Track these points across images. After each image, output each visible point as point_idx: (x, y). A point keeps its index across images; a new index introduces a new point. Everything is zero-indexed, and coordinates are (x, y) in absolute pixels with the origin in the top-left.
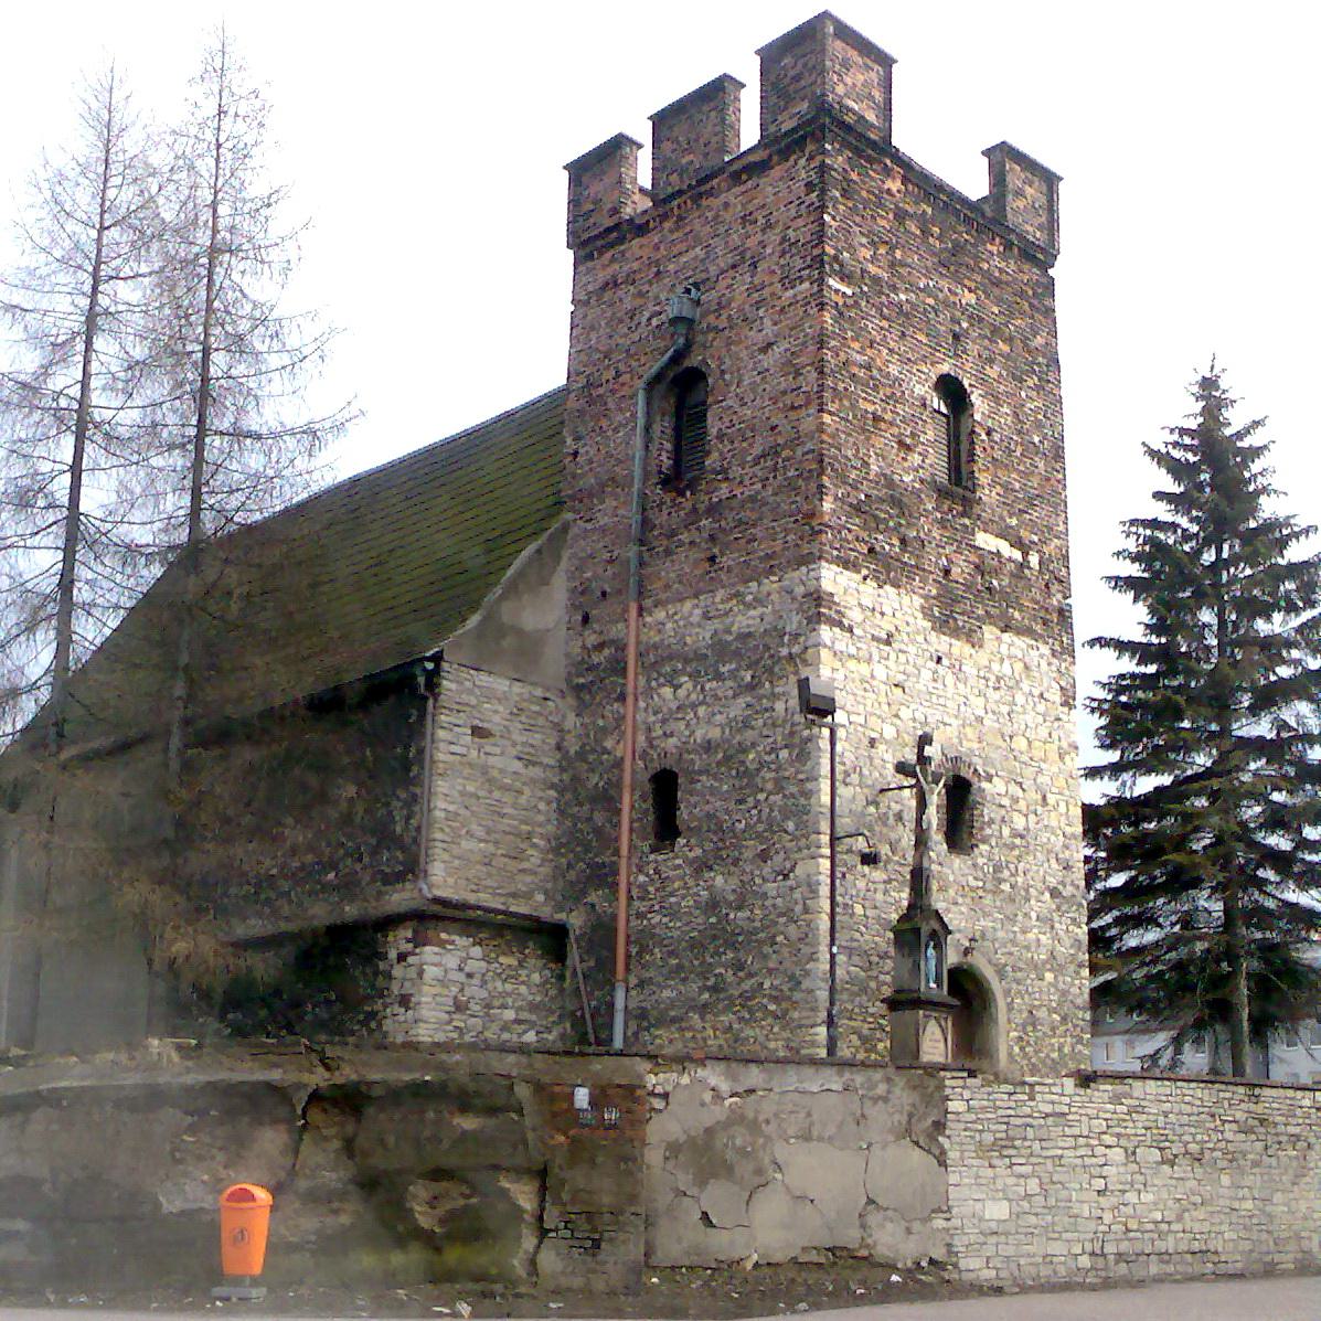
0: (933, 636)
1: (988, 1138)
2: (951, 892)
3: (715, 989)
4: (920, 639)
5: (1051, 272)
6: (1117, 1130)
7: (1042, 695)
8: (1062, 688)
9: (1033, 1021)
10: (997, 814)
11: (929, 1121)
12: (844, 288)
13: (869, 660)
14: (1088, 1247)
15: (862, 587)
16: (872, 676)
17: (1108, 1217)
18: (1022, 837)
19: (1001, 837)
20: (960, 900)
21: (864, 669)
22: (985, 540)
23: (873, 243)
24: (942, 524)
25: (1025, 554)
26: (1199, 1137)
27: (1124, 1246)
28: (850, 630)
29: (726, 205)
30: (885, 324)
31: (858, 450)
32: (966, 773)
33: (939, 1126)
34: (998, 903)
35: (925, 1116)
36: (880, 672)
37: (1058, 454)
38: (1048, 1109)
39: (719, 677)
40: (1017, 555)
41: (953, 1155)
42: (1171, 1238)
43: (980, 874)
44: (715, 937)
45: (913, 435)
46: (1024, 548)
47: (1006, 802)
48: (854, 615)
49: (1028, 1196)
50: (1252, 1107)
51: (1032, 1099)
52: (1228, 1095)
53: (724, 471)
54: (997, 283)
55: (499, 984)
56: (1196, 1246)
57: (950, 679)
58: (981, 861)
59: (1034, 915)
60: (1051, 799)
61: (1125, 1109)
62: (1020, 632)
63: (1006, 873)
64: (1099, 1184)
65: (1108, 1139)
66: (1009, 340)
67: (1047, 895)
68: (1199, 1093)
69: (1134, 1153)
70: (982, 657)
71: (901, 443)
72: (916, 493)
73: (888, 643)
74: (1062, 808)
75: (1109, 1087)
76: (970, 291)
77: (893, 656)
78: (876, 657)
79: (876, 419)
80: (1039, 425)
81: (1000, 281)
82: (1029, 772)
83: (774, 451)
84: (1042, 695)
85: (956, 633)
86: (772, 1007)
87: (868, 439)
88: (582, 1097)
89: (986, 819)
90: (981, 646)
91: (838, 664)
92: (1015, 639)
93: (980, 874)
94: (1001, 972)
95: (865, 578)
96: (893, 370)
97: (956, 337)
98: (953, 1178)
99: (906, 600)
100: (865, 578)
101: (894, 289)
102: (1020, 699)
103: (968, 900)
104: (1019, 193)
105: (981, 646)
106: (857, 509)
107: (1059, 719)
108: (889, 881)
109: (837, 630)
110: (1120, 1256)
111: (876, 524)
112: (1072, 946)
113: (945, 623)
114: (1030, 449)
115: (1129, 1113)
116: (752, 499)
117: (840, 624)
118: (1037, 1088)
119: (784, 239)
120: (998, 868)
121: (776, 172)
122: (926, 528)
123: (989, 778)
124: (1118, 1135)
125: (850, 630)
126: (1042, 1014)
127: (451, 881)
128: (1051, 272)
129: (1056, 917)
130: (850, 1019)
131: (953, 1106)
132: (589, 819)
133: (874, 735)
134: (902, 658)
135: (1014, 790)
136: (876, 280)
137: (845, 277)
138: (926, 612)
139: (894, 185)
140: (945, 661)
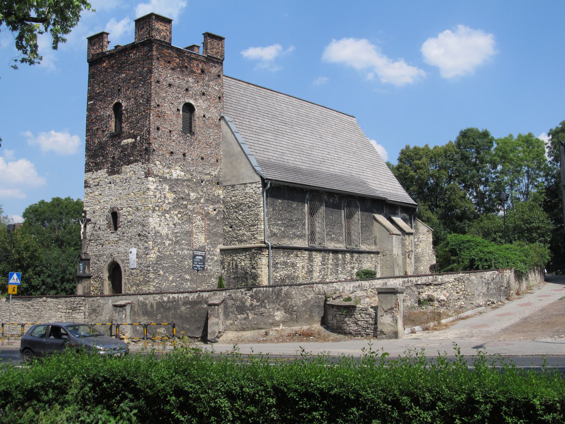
0: (109, 178)
21: (93, 195)
40: (134, 140)
72: (107, 142)
73: (98, 185)
79: (97, 129)
92: (132, 166)
120: (123, 233)
123: (122, 209)
136: (99, 93)
140: (112, 182)
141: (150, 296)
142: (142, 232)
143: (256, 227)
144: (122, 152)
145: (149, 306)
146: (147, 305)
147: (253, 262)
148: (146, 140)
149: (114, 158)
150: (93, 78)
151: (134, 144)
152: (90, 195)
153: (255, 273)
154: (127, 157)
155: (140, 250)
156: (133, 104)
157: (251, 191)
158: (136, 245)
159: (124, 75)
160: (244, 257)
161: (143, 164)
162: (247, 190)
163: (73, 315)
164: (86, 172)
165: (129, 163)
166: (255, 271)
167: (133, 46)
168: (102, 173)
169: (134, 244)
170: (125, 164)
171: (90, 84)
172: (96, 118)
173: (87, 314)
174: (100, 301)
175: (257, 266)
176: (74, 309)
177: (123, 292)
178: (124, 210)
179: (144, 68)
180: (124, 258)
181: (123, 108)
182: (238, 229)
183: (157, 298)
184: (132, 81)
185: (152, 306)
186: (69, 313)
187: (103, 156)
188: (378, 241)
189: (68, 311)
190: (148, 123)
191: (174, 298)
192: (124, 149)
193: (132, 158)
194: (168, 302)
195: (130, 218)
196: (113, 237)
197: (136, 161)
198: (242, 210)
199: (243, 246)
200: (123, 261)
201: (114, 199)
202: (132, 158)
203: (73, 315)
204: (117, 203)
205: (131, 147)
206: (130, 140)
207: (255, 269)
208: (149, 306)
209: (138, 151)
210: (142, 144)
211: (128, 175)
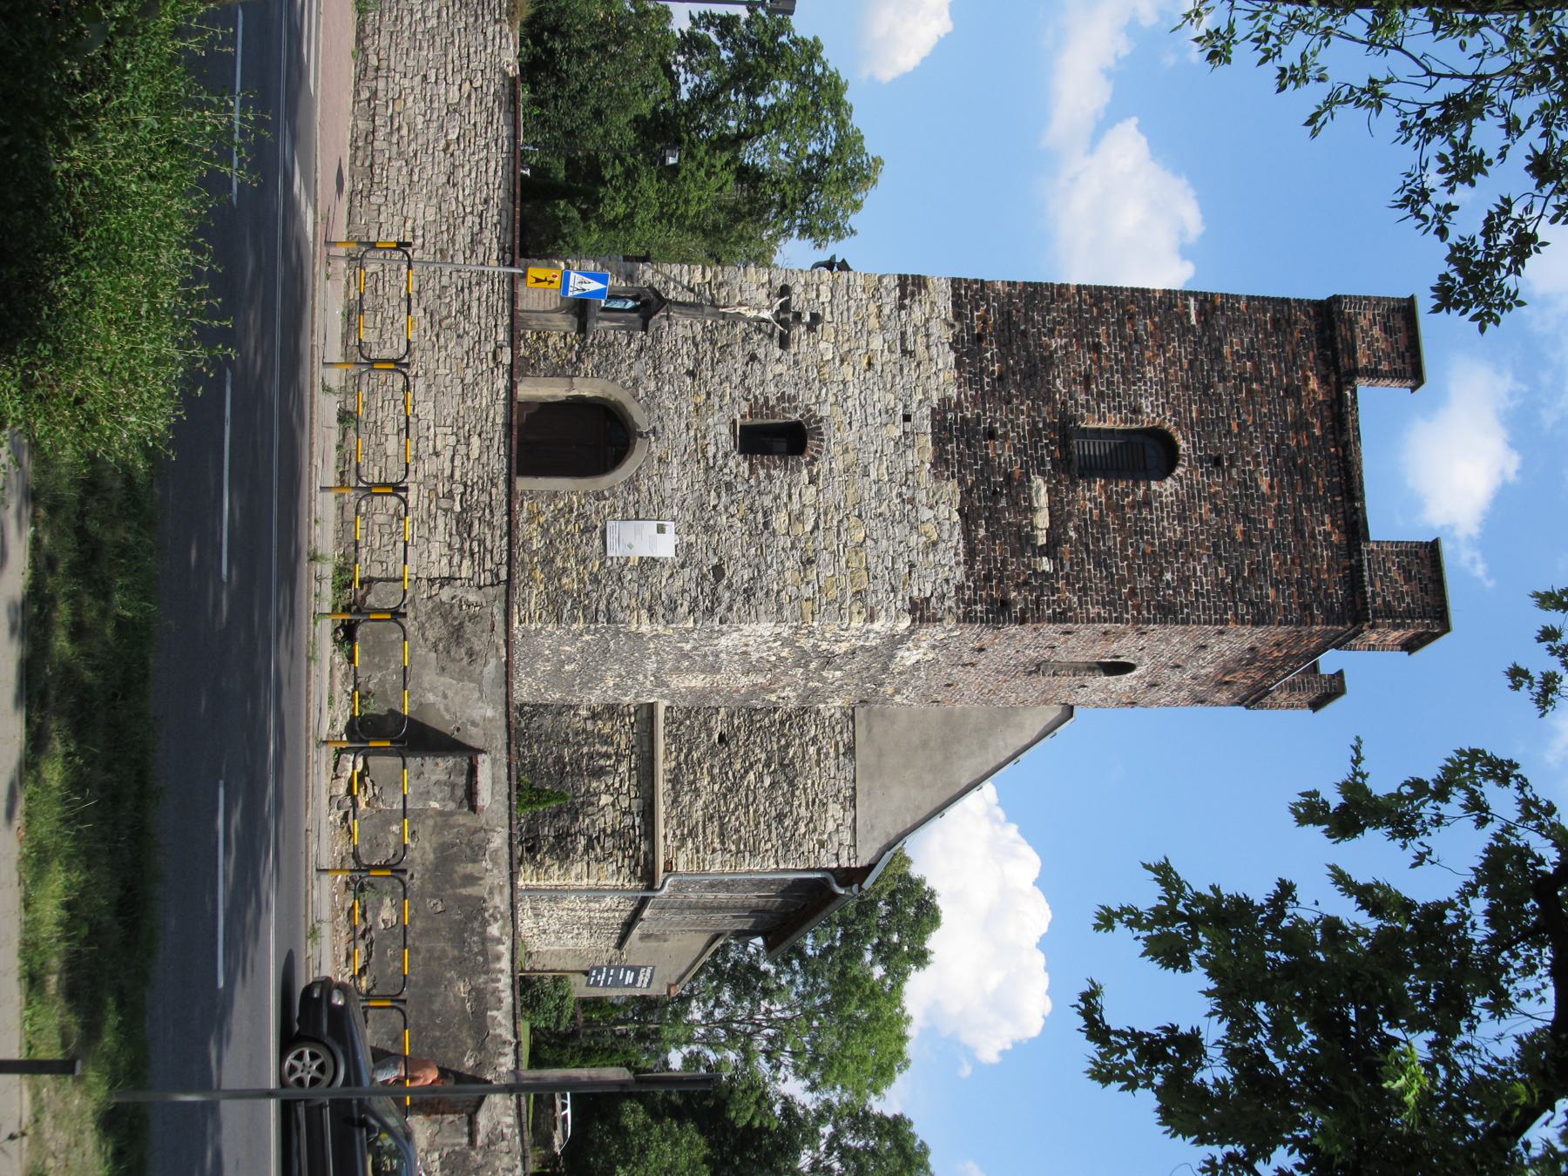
0: (926, 411)
13: (882, 328)
17: (406, 83)
18: (766, 525)
20: (692, 433)
21: (873, 322)
22: (1039, 484)
24: (1035, 431)
25: (1050, 550)
28: (902, 307)
31: (1059, 323)
40: (1042, 541)
42: (385, 145)
45: (1101, 394)
46: (1050, 550)
47: (795, 506)
54: (1299, 532)
59: (693, 538)
62: (967, 534)
65: (467, 86)
67: (715, 561)
70: (925, 476)
72: (1048, 398)
73: (905, 352)
78: (888, 336)
79: (1096, 348)
80: (1184, 581)
81: (1303, 536)
85: (937, 441)
89: (775, 473)
92: (958, 529)
100: (952, 326)
101: (1223, 379)
108: (696, 345)
110: (374, 94)
111: (1005, 345)
113: (938, 416)
117: (903, 296)
120: (729, 486)
125: (902, 307)
136: (1219, 354)
138: (944, 401)
140: (908, 426)
141: (506, 873)
142: (729, 587)
143: (717, 846)
144: (1009, 477)
145: (470, 868)
146: (475, 861)
147: (609, 843)
148: (1037, 602)
149: (991, 434)
150: (1275, 321)
151: (1023, 541)
152: (873, 308)
153: (574, 850)
154: (988, 505)
155: (666, 574)
156: (1162, 535)
157: (831, 826)
158: (686, 551)
159: (1264, 488)
160: (625, 804)
162: (835, 810)
163: (441, 521)
164: (956, 283)
165: (968, 517)
166: (581, 848)
167: (1355, 527)
168: (940, 375)
169: (690, 545)
170: (967, 493)
171: (1260, 303)
172: (1138, 339)
173: (445, 594)
174: (493, 662)
175: (597, 860)
176: (463, 525)
177: (522, 484)
179: (1275, 584)
180: (644, 489)
181: (1154, 485)
182: (716, 771)
183: (497, 900)
184: (1239, 527)
185: (471, 880)
186: (450, 495)
187: (1000, 378)
188: (653, 944)
190: (1093, 611)
191: (498, 958)
192: (1016, 487)
193: (982, 532)
194: (485, 939)
195: (780, 521)
196: (721, 435)
197: (971, 553)
198: (773, 785)
199: (662, 786)
200: (632, 484)
201: (850, 437)
205: (1020, 527)
206: (1042, 520)
207: (586, 851)
208: (470, 868)
209: (1004, 562)
210: (1026, 583)
211: (926, 514)
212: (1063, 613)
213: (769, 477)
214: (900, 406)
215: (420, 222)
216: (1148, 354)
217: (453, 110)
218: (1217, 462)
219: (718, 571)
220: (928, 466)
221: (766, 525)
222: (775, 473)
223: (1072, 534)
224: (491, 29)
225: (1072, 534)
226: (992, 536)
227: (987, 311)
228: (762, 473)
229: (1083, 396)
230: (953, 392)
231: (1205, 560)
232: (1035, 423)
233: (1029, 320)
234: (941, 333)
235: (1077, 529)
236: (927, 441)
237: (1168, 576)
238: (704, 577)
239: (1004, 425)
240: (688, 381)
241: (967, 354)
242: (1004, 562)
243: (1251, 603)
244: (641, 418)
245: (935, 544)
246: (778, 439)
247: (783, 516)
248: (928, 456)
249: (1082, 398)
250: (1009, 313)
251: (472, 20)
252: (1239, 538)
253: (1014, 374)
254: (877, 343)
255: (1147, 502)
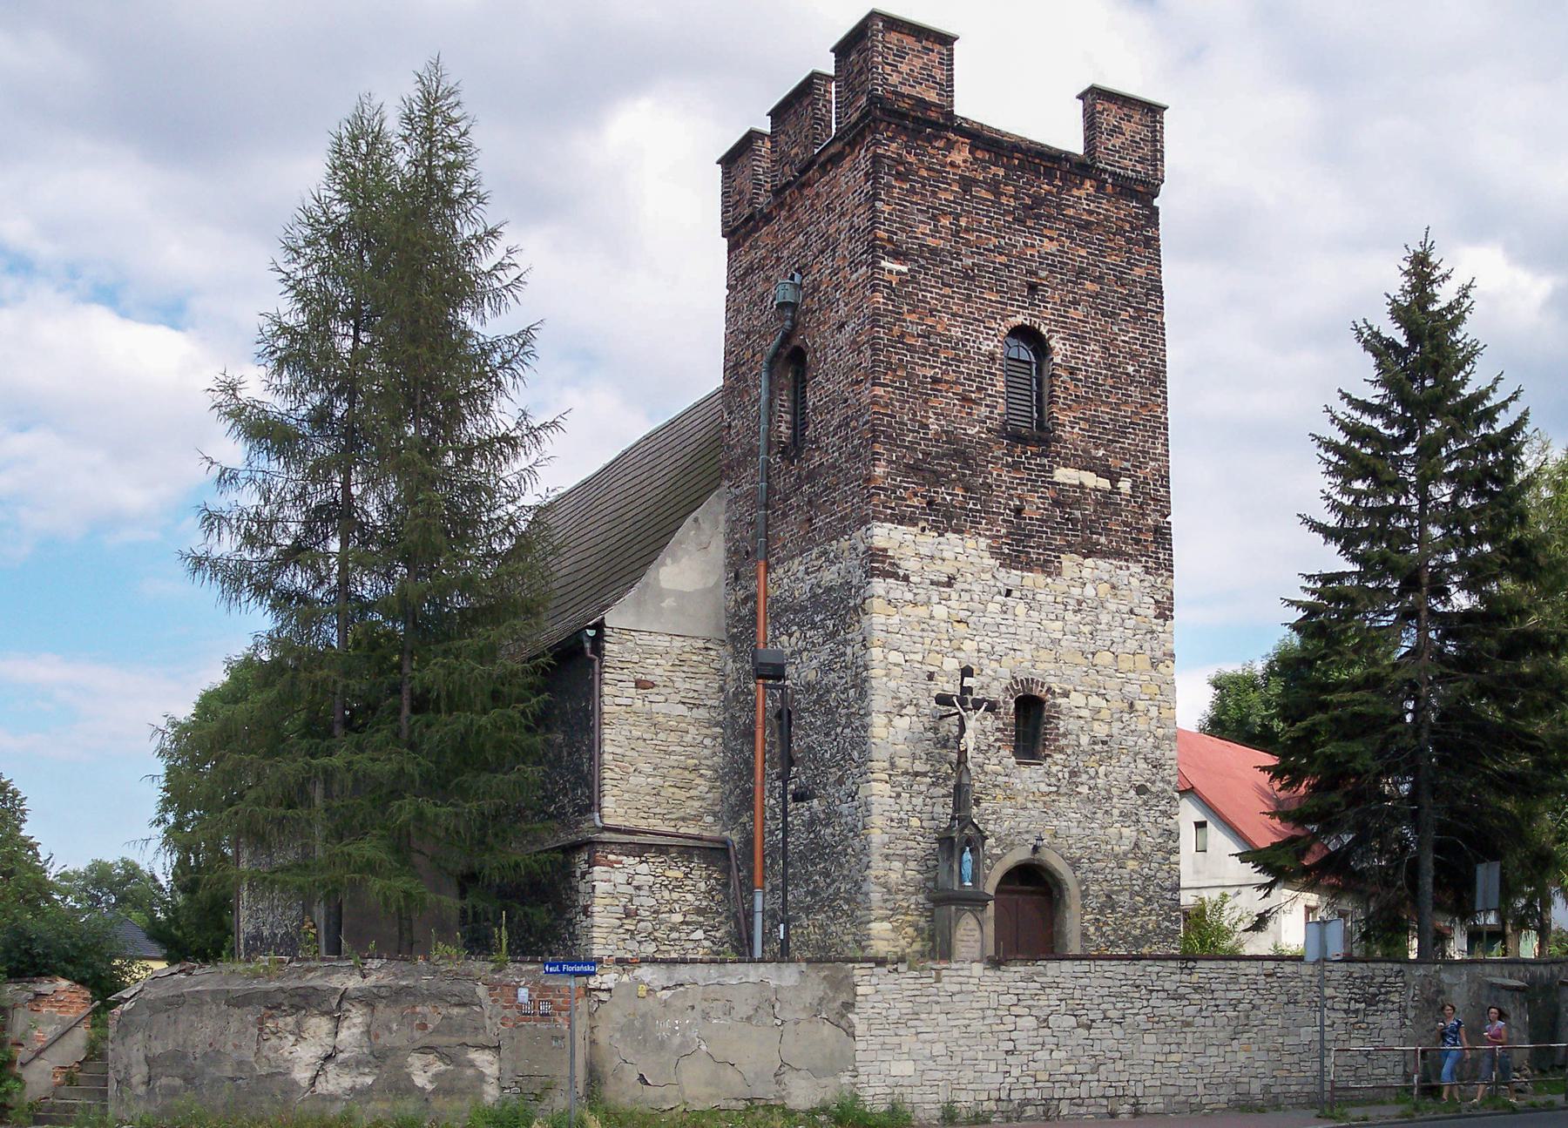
0: (1002, 573)
1: (894, 1015)
2: (1020, 800)
3: (813, 894)
4: (988, 576)
5: (1156, 202)
6: (1030, 1002)
7: (1131, 612)
8: (1157, 602)
9: (1110, 903)
10: (1073, 725)
11: (839, 1003)
12: (897, 267)
13: (928, 603)
14: (994, 1095)
15: (920, 539)
16: (932, 617)
17: (1015, 1072)
18: (1104, 743)
19: (1079, 745)
20: (1030, 805)
21: (922, 612)
22: (1064, 475)
23: (934, 218)
24: (1015, 466)
25: (1114, 478)
26: (1119, 1005)
27: (1030, 1094)
28: (906, 578)
29: (818, 195)
30: (947, 291)
31: (915, 414)
32: (1037, 691)
33: (849, 1006)
34: (1074, 805)
35: (834, 999)
36: (940, 611)
37: (1157, 378)
38: (956, 988)
39: (814, 626)
40: (1105, 484)
41: (860, 1029)
43: (1053, 780)
44: (813, 850)
45: (979, 389)
46: (1114, 478)
47: (1085, 713)
48: (910, 565)
49: (933, 1058)
50: (1185, 977)
51: (938, 980)
52: (1156, 969)
53: (816, 441)
54: (1087, 226)
55: (666, 894)
56: (1111, 1092)
57: (1021, 609)
58: (1054, 769)
59: (1116, 812)
60: (1140, 705)
61: (1038, 985)
62: (1105, 555)
63: (1084, 777)
64: (1010, 1045)
66: (1099, 279)
67: (1132, 792)
68: (1122, 969)
69: (1046, 1020)
70: (1060, 585)
71: (965, 399)
73: (949, 584)
74: (1154, 712)
75: (1021, 969)
76: (1052, 239)
77: (954, 596)
78: (935, 599)
79: (935, 380)
80: (1134, 356)
81: (1089, 223)
82: (1111, 684)
83: (845, 423)
84: (1131, 612)
85: (1028, 566)
86: (846, 907)
87: (926, 402)
88: (523, 994)
89: (1062, 730)
90: (1059, 574)
91: (892, 610)
92: (1100, 562)
93: (1053, 780)
94: (1075, 864)
95: (923, 529)
96: (956, 332)
97: (1033, 288)
98: (860, 1046)
99: (971, 543)
100: (923, 529)
102: (1105, 618)
103: (1040, 805)
104: (1116, 131)
105: (1059, 574)
106: (914, 469)
107: (1153, 632)
109: (891, 580)
111: (937, 479)
112: (1161, 836)
113: (1012, 560)
114: (1121, 381)
115: (1043, 988)
116: (833, 466)
117: (895, 576)
118: (944, 972)
119: (852, 227)
120: (1073, 774)
121: (847, 163)
122: (999, 474)
123: (1066, 695)
124: (1029, 1007)
126: (1124, 898)
127: (621, 811)
128: (1156, 202)
129: (1142, 812)
130: (906, 914)
131: (860, 990)
132: (741, 751)
133: (932, 669)
134: (966, 596)
135: (1095, 701)
137: (897, 255)
138: (995, 552)
139: (960, 156)
140: (1016, 594)
142: (1153, 783)
151: (1107, 501)
152: (908, 609)
161: (1147, 571)
170: (1070, 548)
173: (1411, 1014)
176: (1371, 1001)
178: (1077, 699)
186: (1357, 1011)
189: (1354, 1006)
193: (1103, 540)
195: (1101, 730)
196: (1030, 778)
197: (1118, 554)
200: (1075, 864)
202: (1103, 540)
203: (1370, 1019)
204: (1046, 674)
206: (1090, 479)
209: (1126, 524)
211: (1089, 591)
212: (1162, 477)
213: (1065, 735)
214: (998, 598)
215: (1158, 1048)
216: (939, 329)
217: (1044, 1022)
218: (1033, 288)
219: (1141, 790)
220: (1049, 580)
221: (1104, 743)
222: (1062, 730)
223: (1101, 453)
224: (948, 987)
225: (1101, 453)
226: (1107, 531)
227: (906, 489)
228: (1063, 742)
229: (983, 409)
230: (983, 542)
231: (1116, 329)
232: (1007, 465)
233: (911, 448)
234: (928, 542)
235: (1097, 447)
236: (1030, 578)
237: (1130, 369)
238: (1145, 803)
239: (1011, 497)
240: (984, 805)
241: (950, 519)
242: (1126, 524)
243: (1147, 295)
244: (1021, 855)
245: (1113, 587)
246: (1030, 721)
247: (1096, 725)
248: (1040, 578)
249: (985, 411)
250: (907, 465)
251: (936, 1008)
252: (1097, 288)
253: (964, 475)
254: (940, 611)
255: (1072, 372)
